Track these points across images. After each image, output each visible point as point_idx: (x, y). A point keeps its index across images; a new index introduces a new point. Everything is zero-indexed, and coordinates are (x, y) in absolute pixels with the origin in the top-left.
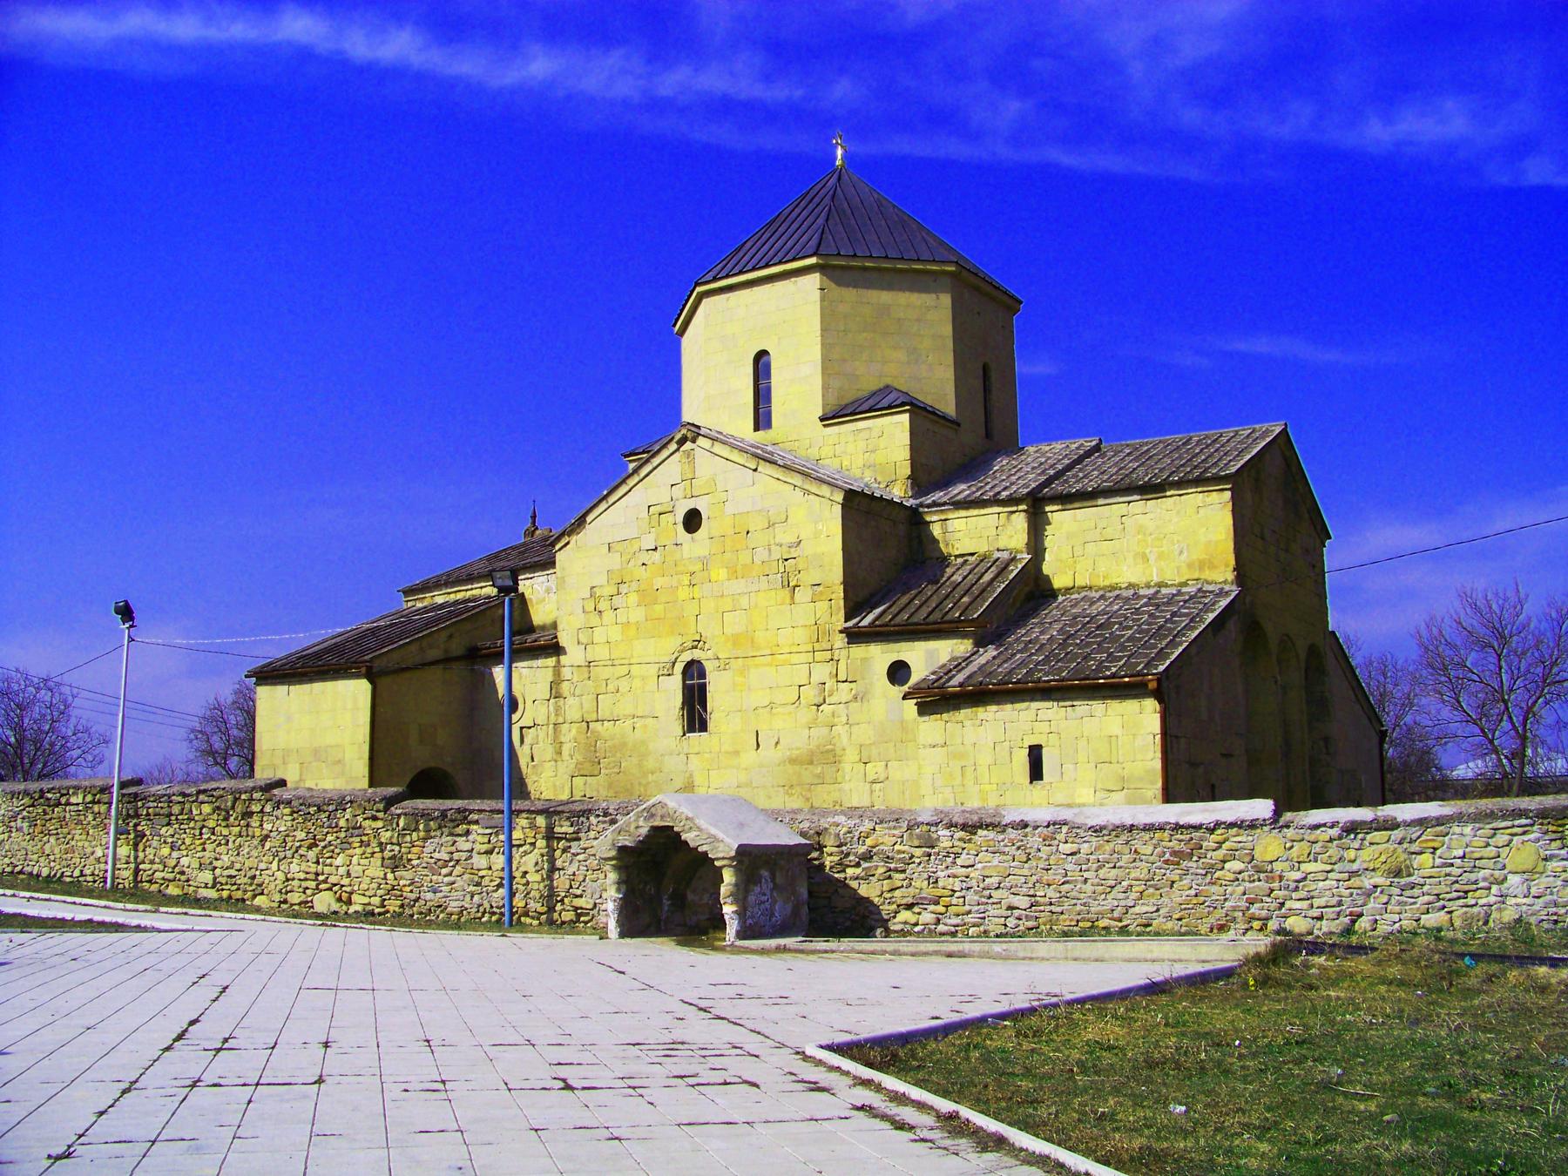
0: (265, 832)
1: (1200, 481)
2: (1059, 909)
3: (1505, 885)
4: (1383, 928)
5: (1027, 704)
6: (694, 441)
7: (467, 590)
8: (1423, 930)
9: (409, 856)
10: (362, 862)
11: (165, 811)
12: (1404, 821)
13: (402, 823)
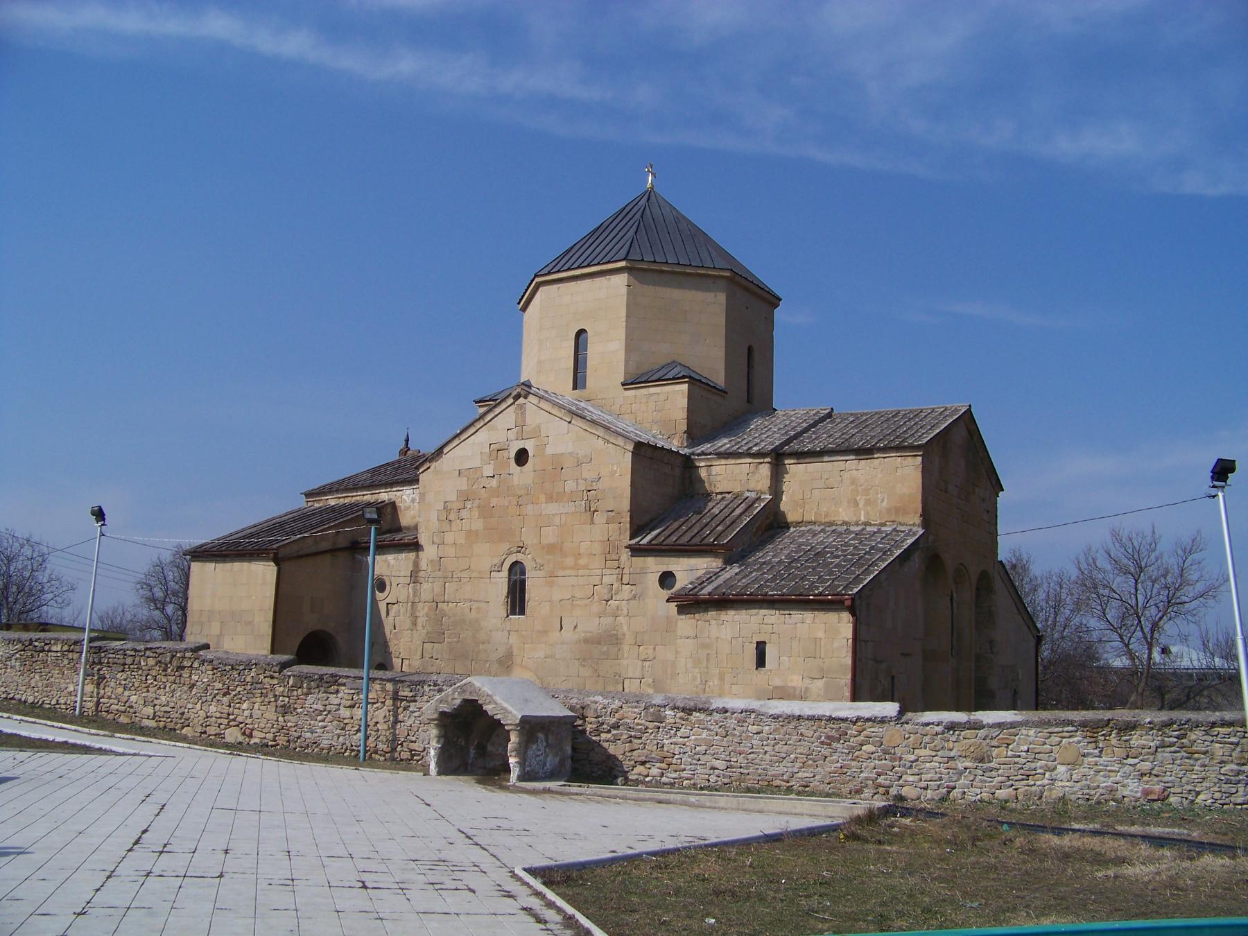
0: (192, 682)
1: (898, 448)
2: (746, 771)
3: (1055, 772)
5: (757, 610)
6: (526, 398)
7: (352, 496)
8: (996, 801)
9: (295, 706)
10: (262, 708)
11: (121, 661)
12: (988, 724)
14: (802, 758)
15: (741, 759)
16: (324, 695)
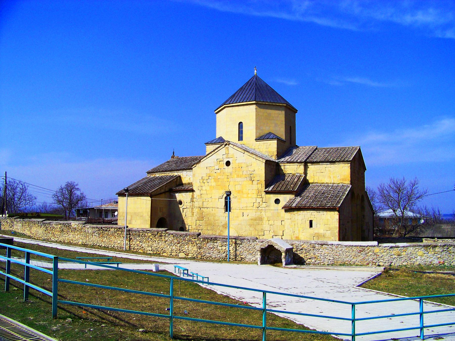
0: (166, 240)
1: (343, 161)
2: (338, 260)
3: (417, 258)
4: (396, 265)
5: (309, 211)
6: (229, 145)
7: (165, 174)
9: (203, 246)
10: (192, 247)
11: (138, 234)
13: (202, 240)
14: (353, 256)
15: (337, 257)
16: (213, 243)
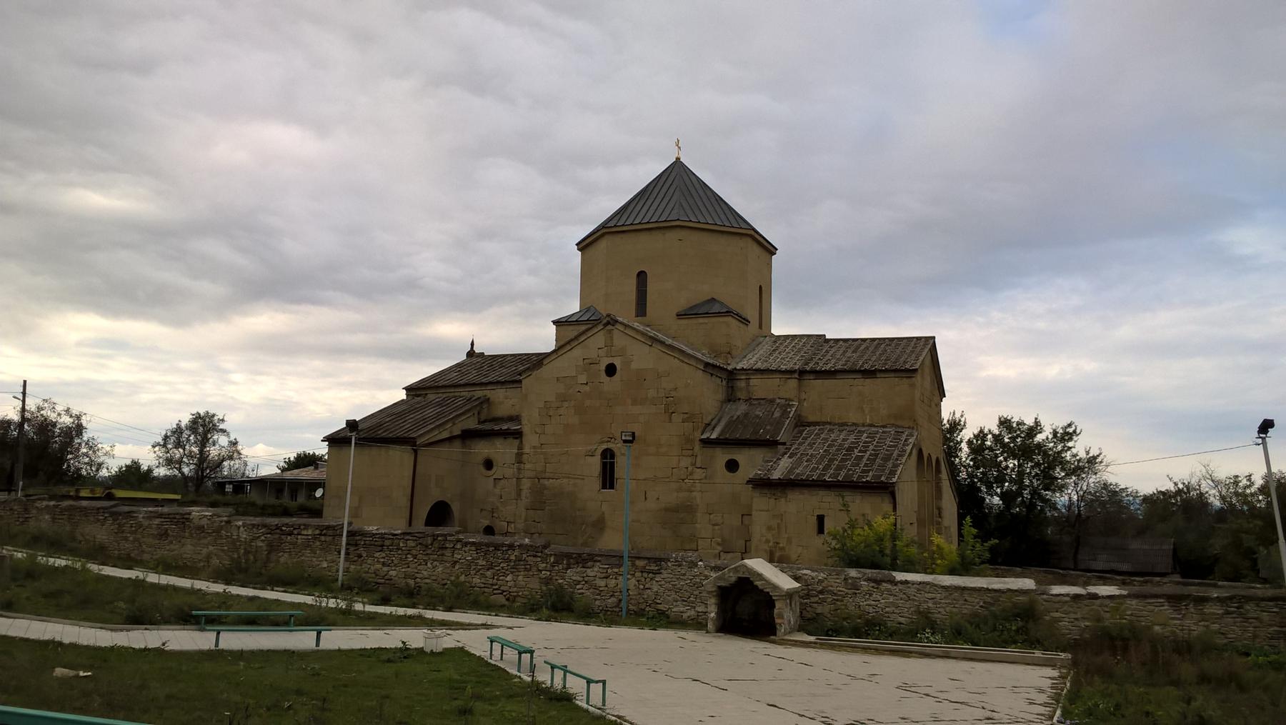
0: (454, 559)
6: (613, 326)
9: (557, 578)
10: (525, 579)
11: (380, 543)
12: (1103, 596)
